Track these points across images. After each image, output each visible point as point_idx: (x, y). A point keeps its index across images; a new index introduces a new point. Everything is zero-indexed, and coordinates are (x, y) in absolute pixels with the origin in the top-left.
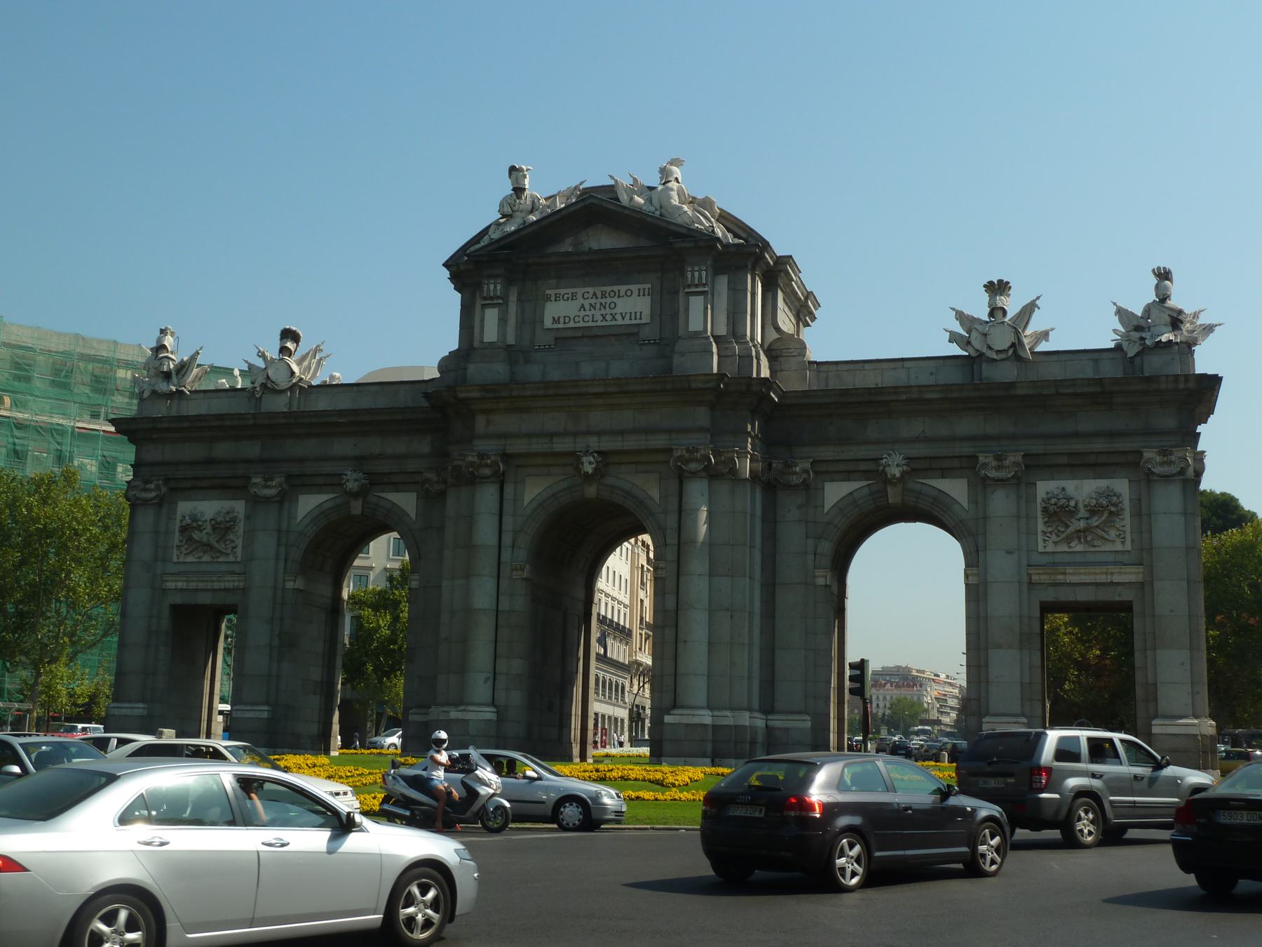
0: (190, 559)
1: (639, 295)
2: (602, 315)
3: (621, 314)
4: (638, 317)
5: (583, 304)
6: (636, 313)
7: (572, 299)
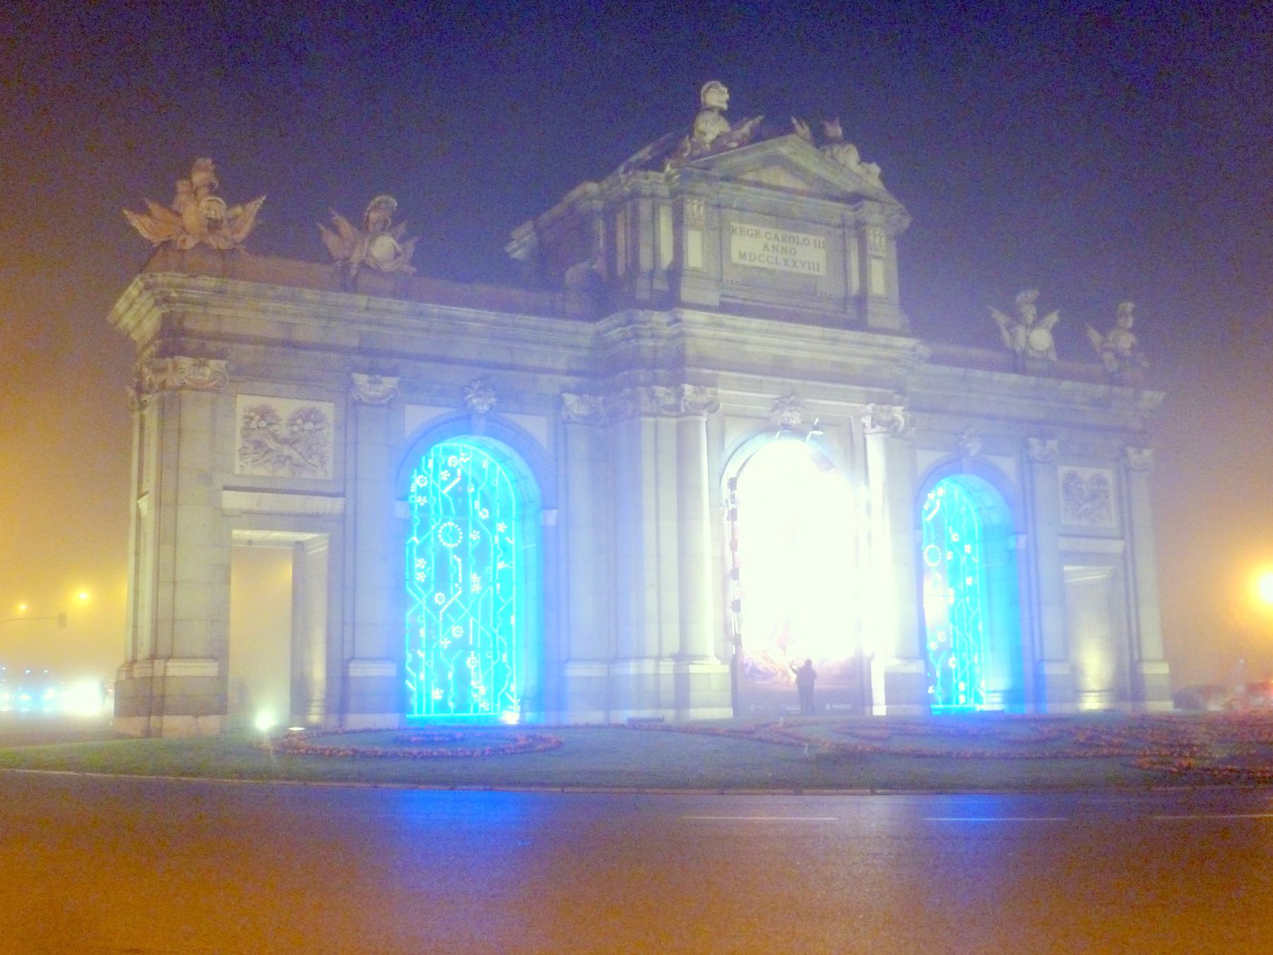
0: (261, 471)
1: (815, 246)
2: (784, 259)
3: (801, 262)
4: (816, 267)
5: (766, 245)
6: (814, 263)
7: (756, 236)
